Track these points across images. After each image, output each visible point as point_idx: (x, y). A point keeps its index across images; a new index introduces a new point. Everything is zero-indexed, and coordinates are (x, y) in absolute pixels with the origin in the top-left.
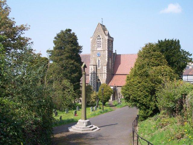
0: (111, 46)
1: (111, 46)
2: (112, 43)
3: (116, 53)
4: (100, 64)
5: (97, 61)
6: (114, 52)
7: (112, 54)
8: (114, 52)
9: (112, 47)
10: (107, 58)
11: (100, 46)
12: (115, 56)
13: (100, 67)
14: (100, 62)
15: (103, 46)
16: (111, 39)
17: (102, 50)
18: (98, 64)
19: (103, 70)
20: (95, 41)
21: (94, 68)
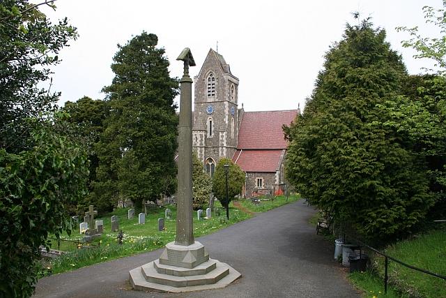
0: (234, 93)
1: (234, 93)
2: (236, 89)
3: (243, 109)
4: (213, 129)
5: (208, 123)
6: (239, 107)
7: (236, 109)
8: (239, 107)
9: (236, 97)
10: (227, 117)
11: (214, 93)
12: (241, 115)
13: (213, 134)
14: (213, 124)
15: (218, 94)
16: (235, 81)
17: (217, 100)
18: (208, 129)
19: (218, 141)
20: (204, 83)
21: (201, 136)
